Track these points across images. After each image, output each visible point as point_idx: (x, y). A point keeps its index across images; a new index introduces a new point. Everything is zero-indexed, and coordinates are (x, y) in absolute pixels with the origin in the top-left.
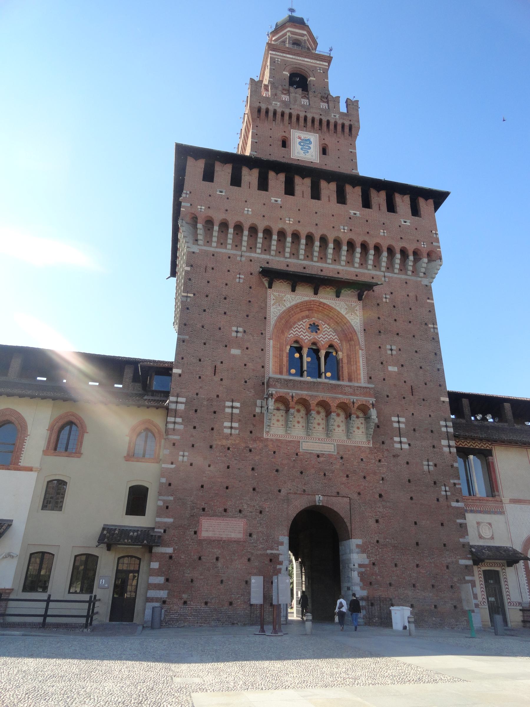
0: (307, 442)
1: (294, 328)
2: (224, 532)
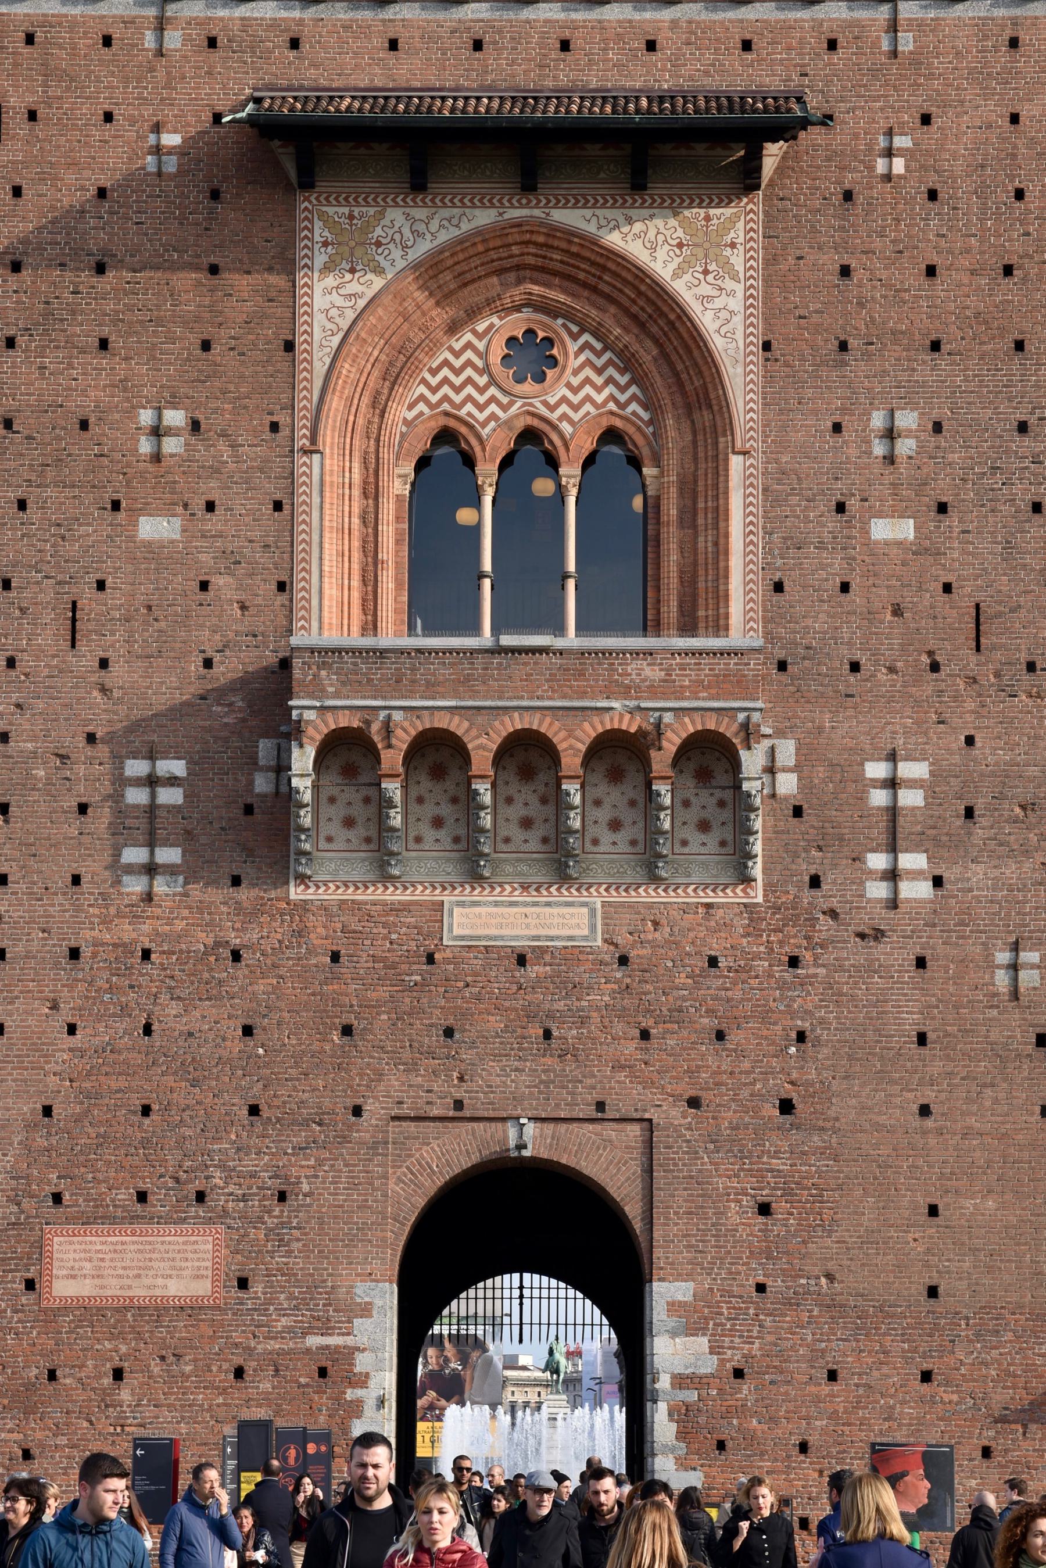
1: (434, 372)
2: (138, 1276)
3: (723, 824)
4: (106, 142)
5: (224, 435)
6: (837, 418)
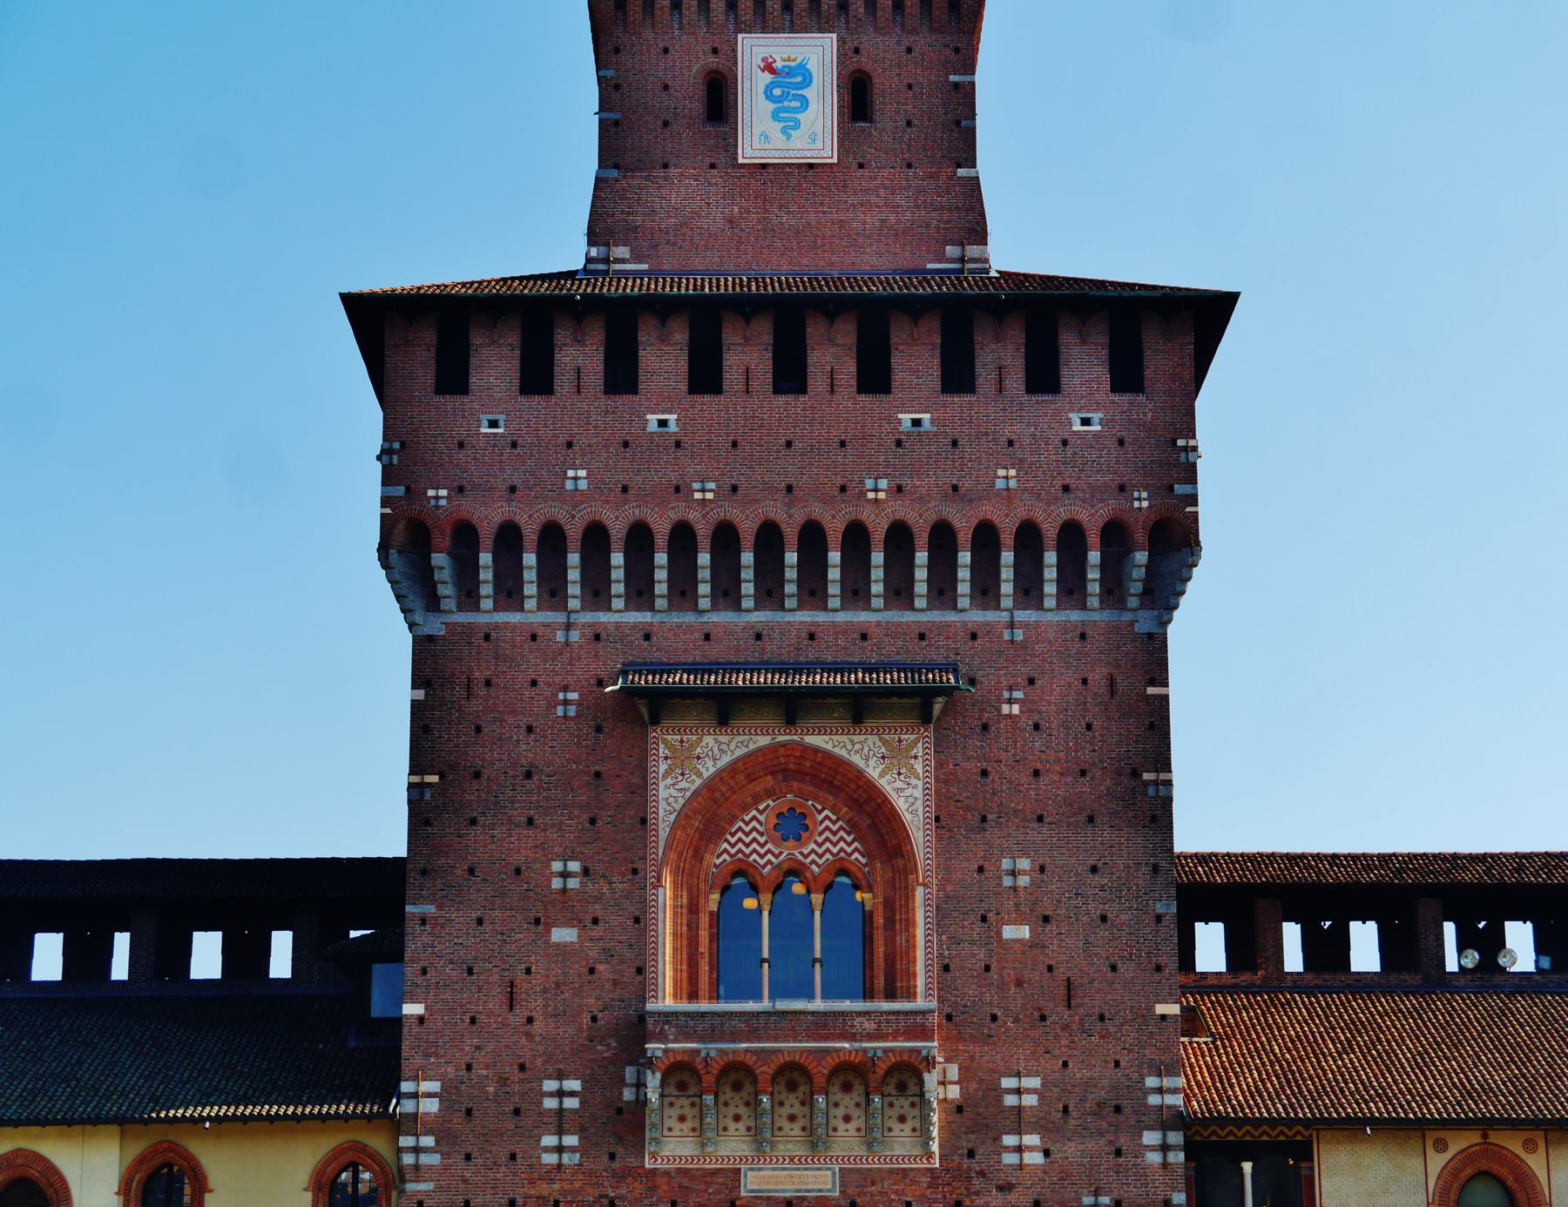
0: (759, 1169)
1: (733, 835)
5: (603, 876)
6: (981, 863)
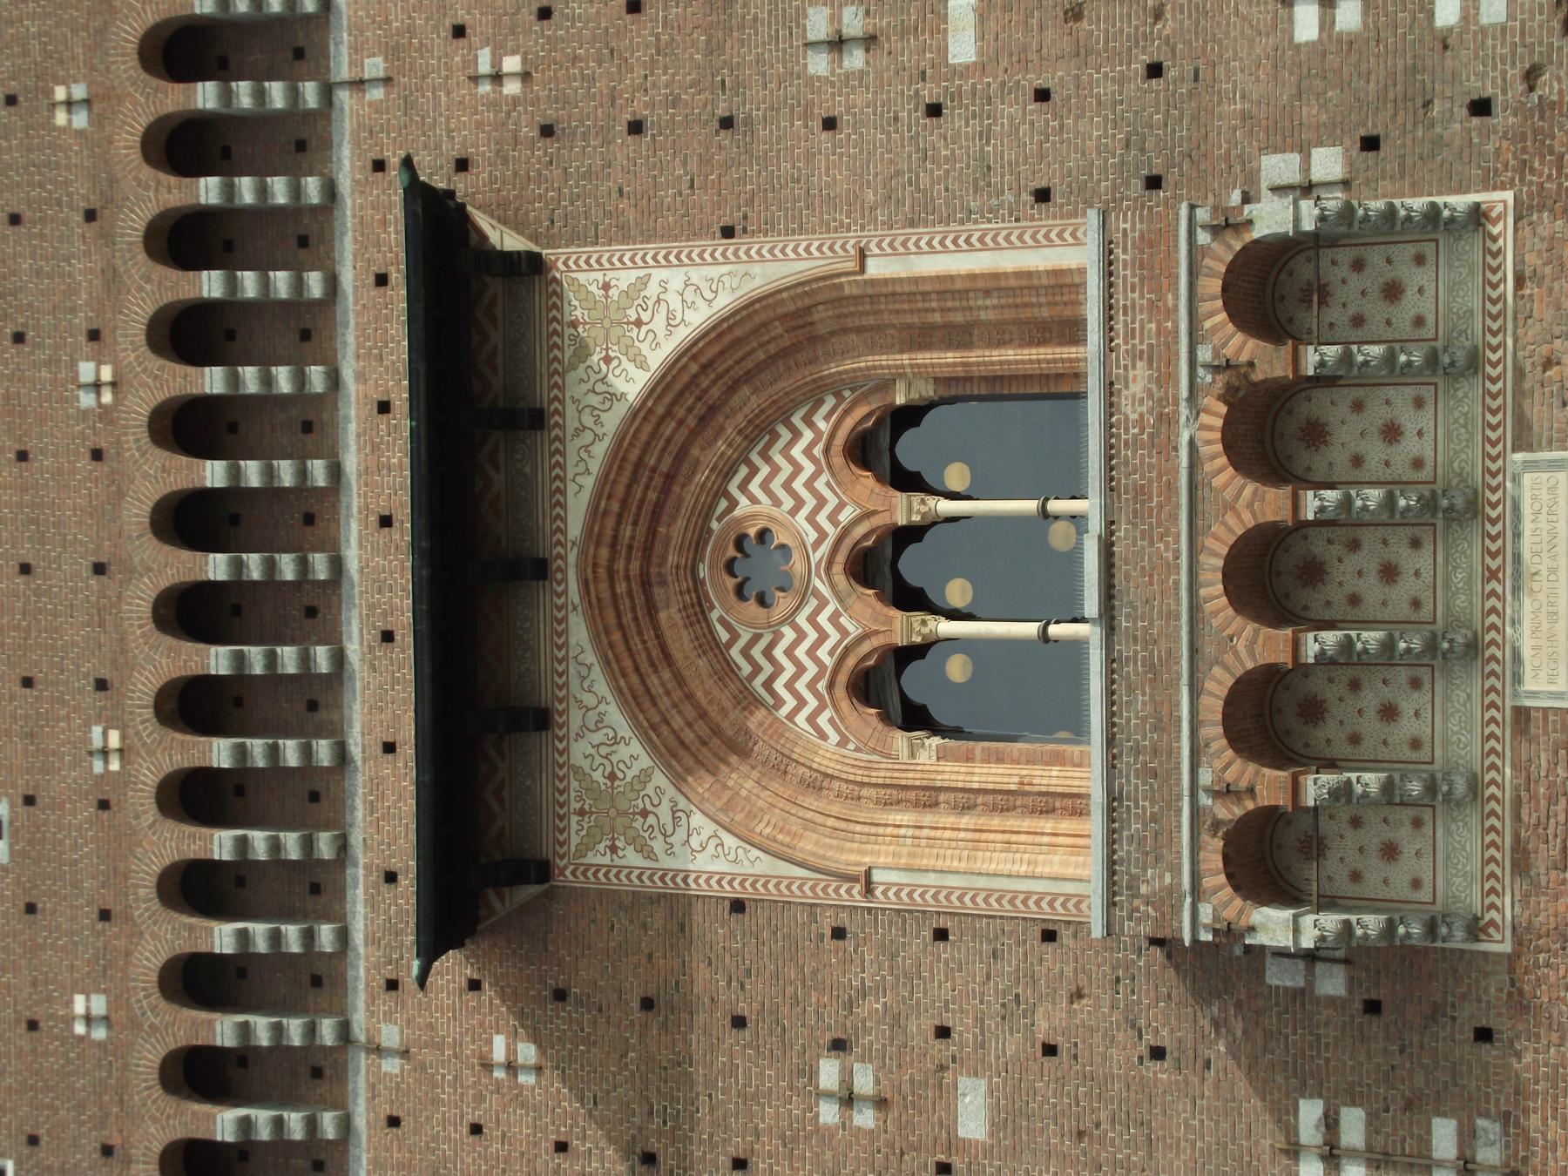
3: (1389, 261)
4: (504, 1135)
5: (850, 1005)
6: (817, 124)
